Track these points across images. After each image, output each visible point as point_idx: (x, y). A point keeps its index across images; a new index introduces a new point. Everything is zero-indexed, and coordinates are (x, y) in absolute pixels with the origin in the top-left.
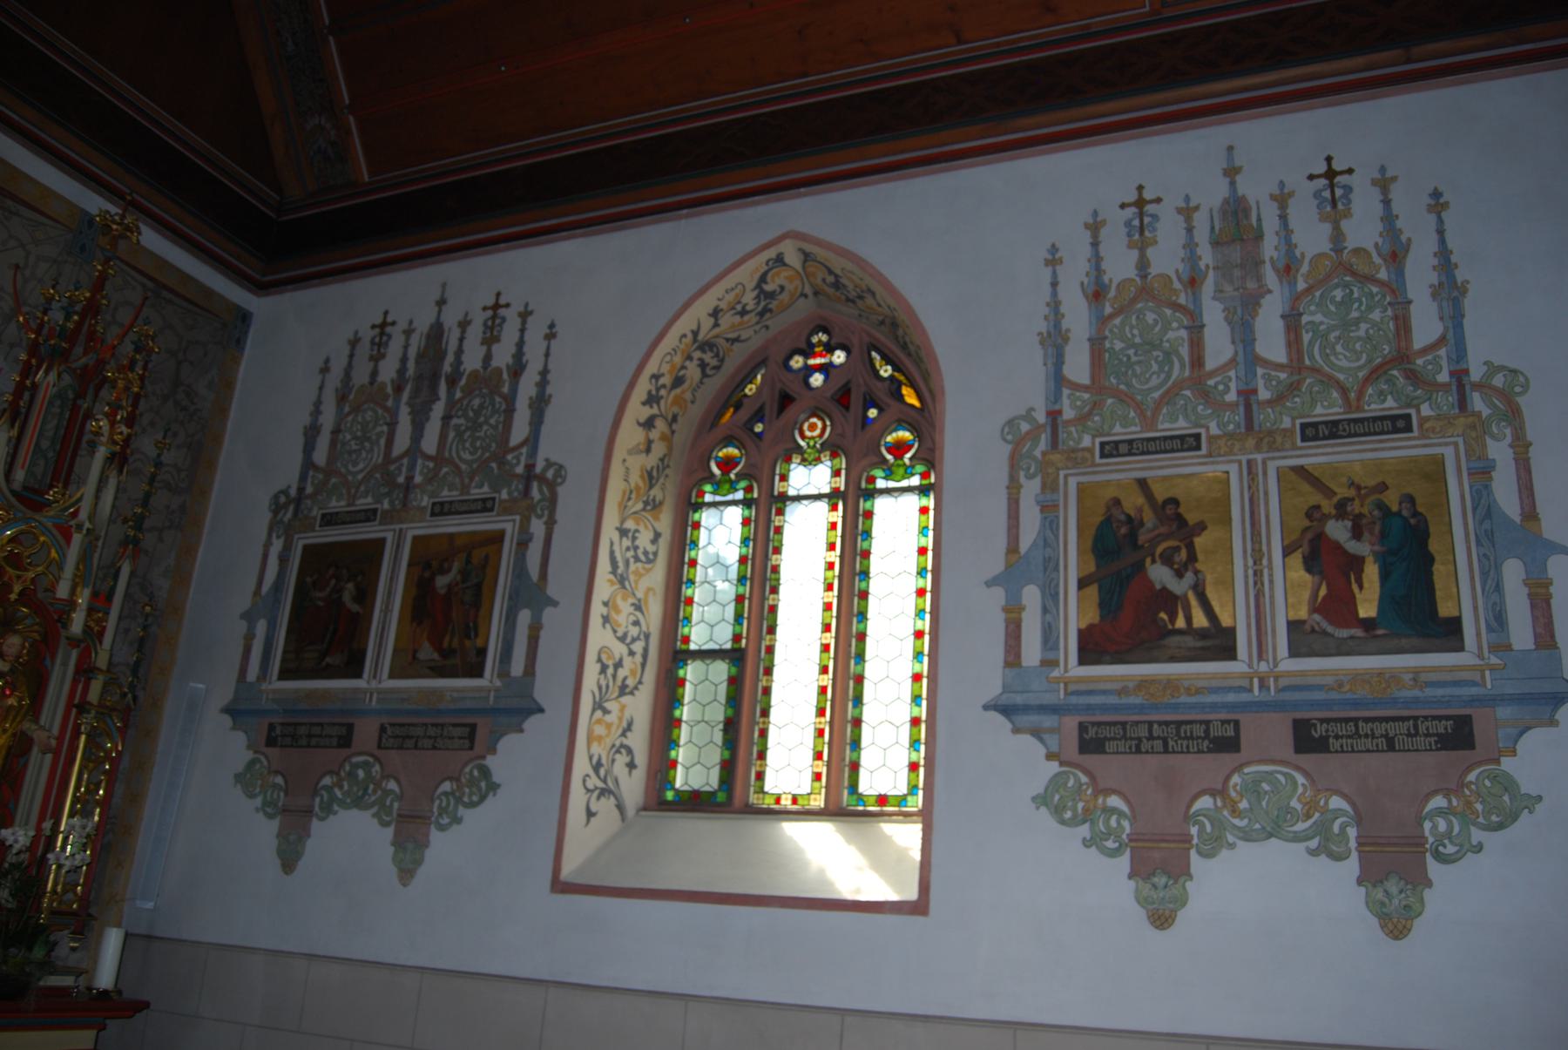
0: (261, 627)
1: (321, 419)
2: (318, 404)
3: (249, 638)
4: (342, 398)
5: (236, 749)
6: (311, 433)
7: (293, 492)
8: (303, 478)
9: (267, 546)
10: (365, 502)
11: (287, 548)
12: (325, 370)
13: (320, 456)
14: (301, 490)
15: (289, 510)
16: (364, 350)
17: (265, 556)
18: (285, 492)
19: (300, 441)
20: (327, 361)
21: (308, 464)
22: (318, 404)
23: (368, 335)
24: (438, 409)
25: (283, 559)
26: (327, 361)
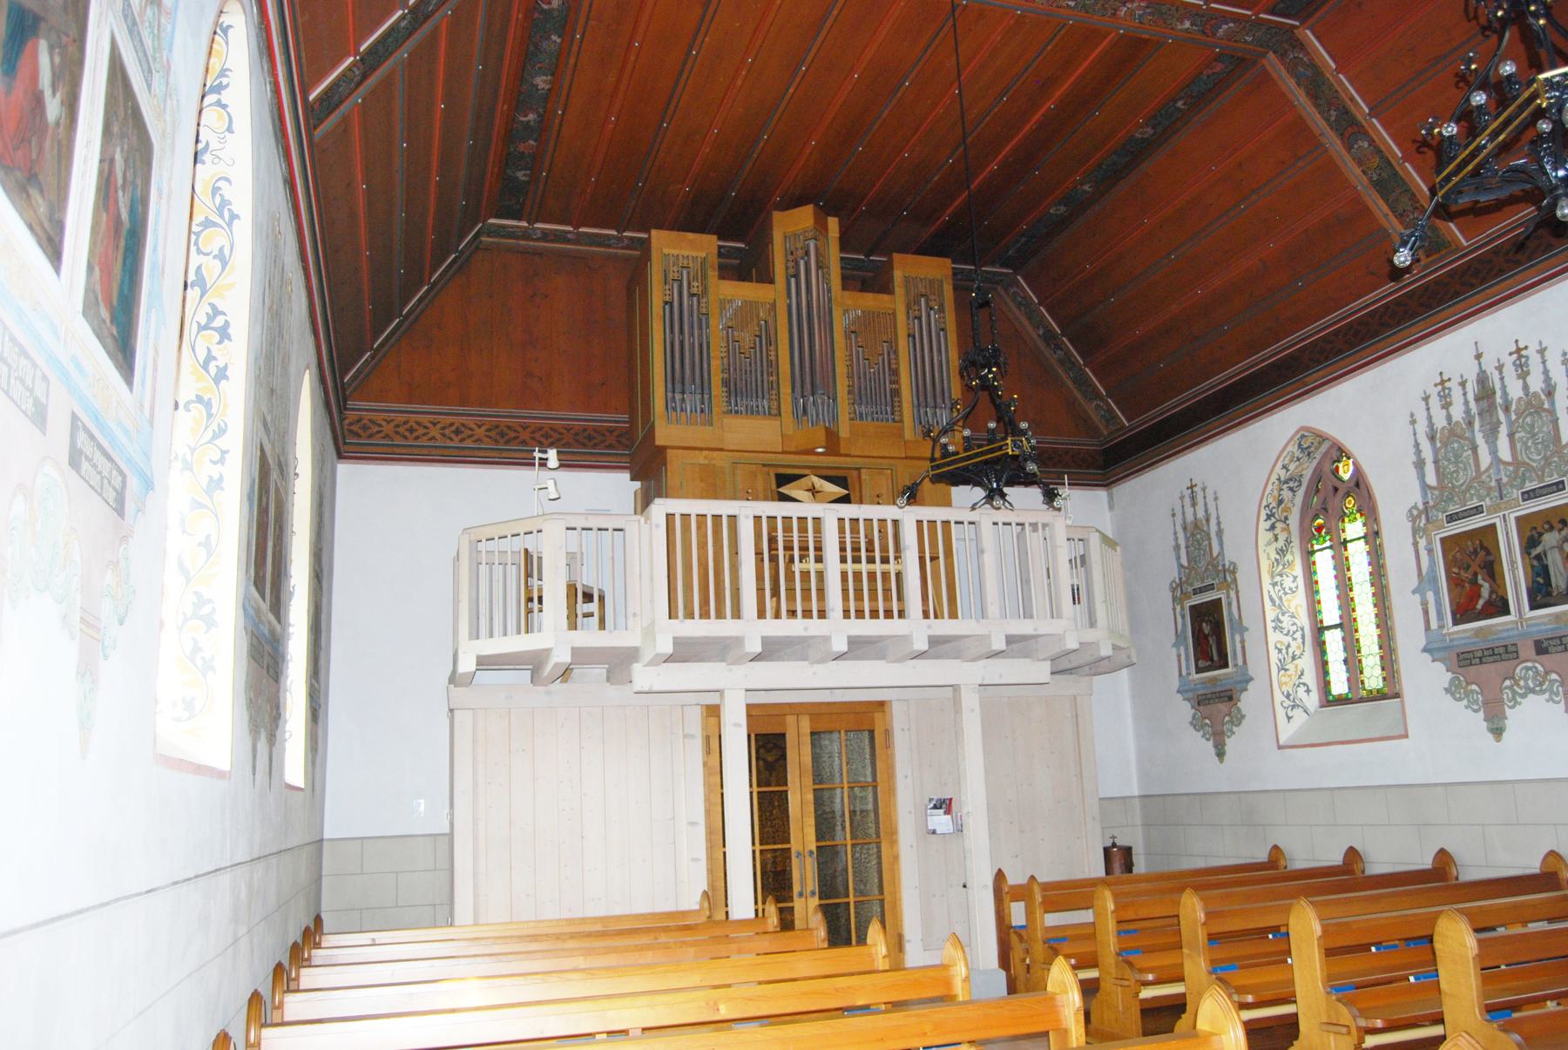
0: (1430, 596)
1: (1423, 455)
2: (1417, 445)
3: (1425, 604)
4: (1432, 438)
5: (1440, 675)
6: (1420, 465)
7: (1421, 507)
8: (1424, 495)
9: (1415, 544)
10: (1474, 503)
11: (1429, 542)
12: (1413, 422)
13: (1431, 479)
14: (1426, 503)
15: (1421, 519)
16: (1435, 402)
17: (1417, 552)
18: (1415, 507)
19: (1413, 472)
20: (1412, 415)
21: (1425, 487)
22: (1417, 445)
23: (1434, 392)
24: (1503, 430)
25: (1430, 551)
26: (1412, 415)
